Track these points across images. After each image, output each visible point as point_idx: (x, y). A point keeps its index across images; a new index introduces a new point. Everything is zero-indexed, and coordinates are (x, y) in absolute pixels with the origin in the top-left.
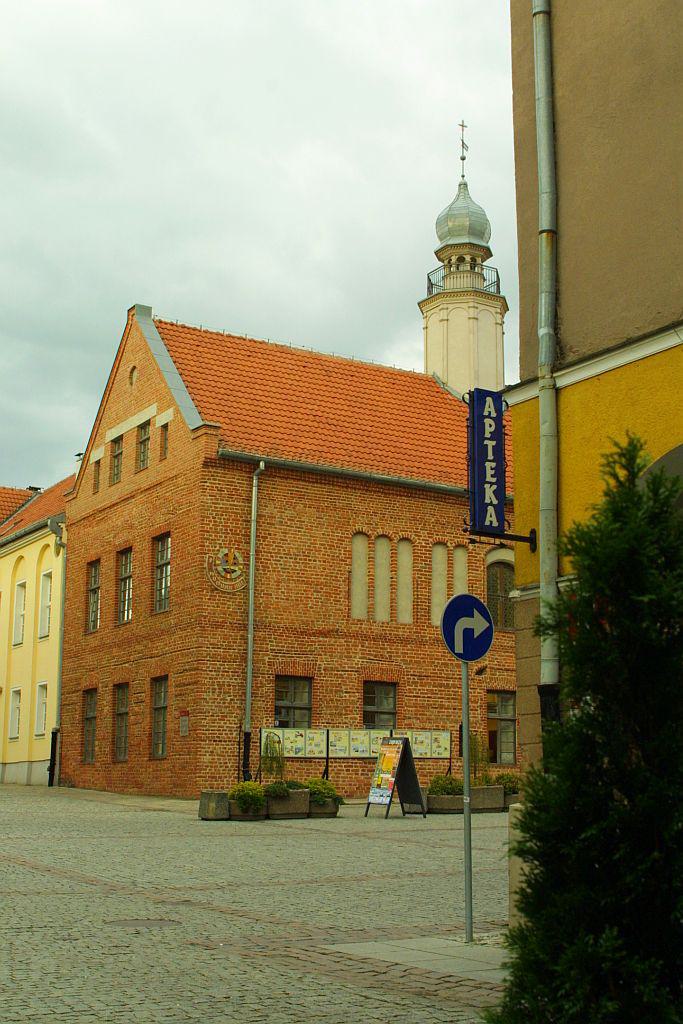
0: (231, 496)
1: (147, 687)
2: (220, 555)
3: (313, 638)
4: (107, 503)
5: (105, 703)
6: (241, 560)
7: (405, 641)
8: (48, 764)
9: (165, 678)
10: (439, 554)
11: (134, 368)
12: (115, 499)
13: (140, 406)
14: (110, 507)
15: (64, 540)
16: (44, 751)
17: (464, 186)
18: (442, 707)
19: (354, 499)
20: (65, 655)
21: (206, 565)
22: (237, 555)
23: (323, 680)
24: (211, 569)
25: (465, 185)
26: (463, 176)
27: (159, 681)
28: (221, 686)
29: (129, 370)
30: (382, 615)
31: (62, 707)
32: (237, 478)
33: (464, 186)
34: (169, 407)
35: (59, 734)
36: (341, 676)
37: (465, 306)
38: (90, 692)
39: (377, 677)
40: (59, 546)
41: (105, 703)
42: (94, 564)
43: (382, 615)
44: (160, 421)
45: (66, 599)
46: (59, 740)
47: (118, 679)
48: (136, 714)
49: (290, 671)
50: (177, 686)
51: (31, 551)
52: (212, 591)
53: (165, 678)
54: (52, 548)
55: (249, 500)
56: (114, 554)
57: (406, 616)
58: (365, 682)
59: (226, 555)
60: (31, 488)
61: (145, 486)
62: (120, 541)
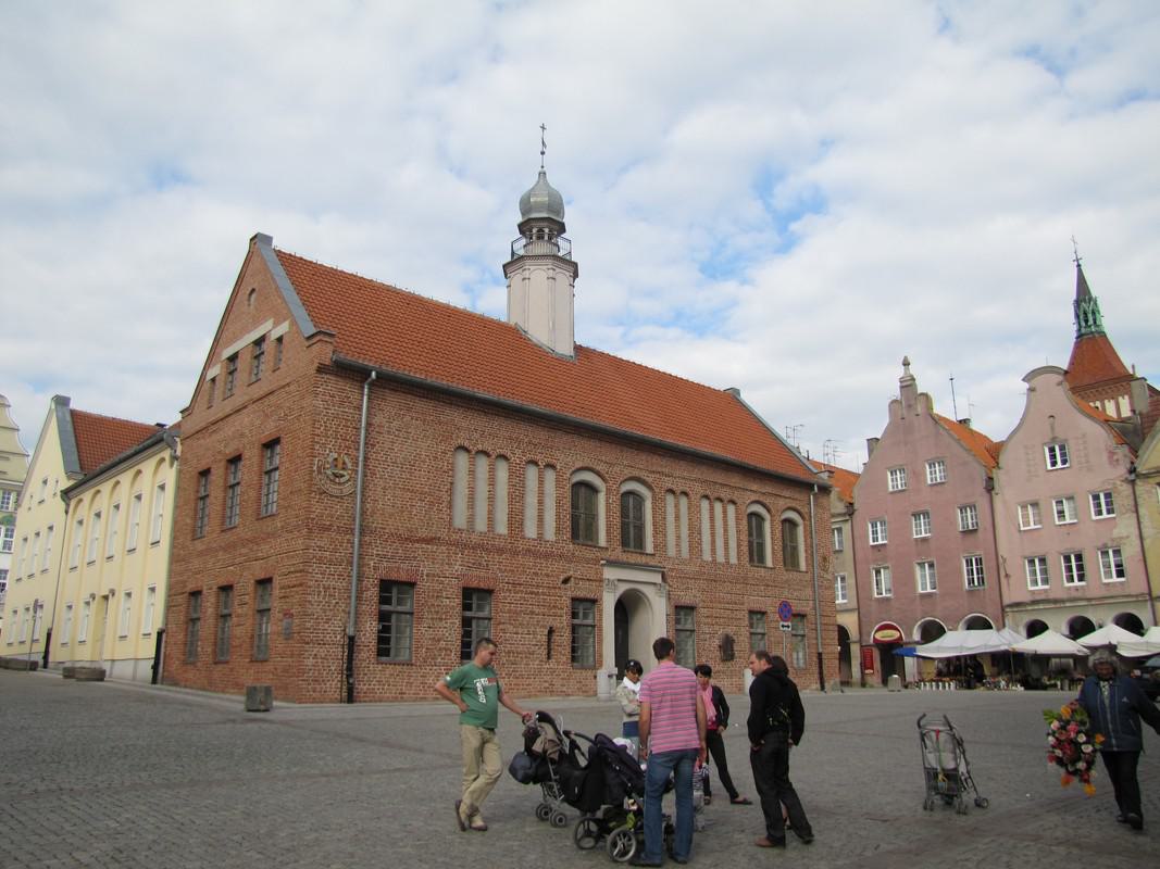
0: (342, 403)
1: (251, 588)
2: (330, 460)
3: (417, 545)
4: (221, 415)
5: (209, 603)
6: (349, 465)
7: (501, 551)
8: (152, 662)
9: (269, 581)
10: (532, 472)
11: (253, 290)
12: (228, 410)
13: (257, 322)
14: (222, 420)
15: (179, 453)
16: (148, 649)
17: (542, 174)
18: (532, 613)
19: (456, 417)
20: (175, 559)
21: (315, 468)
22: (346, 460)
23: (424, 585)
24: (319, 472)
27: (265, 583)
28: (326, 588)
29: (248, 292)
30: (481, 525)
31: (169, 608)
32: (348, 387)
33: (542, 174)
34: (285, 320)
35: (164, 635)
36: (442, 583)
38: (196, 594)
40: (174, 458)
41: (209, 603)
42: (205, 473)
43: (481, 525)
44: (275, 335)
45: (177, 507)
46: (164, 639)
47: (223, 582)
48: (238, 616)
49: (394, 576)
50: (282, 588)
51: (148, 466)
52: (321, 494)
53: (269, 581)
54: (167, 458)
55: (359, 408)
56: (223, 463)
57: (502, 528)
58: (464, 588)
59: (336, 459)
60: (158, 425)
61: (256, 396)
62: (230, 451)
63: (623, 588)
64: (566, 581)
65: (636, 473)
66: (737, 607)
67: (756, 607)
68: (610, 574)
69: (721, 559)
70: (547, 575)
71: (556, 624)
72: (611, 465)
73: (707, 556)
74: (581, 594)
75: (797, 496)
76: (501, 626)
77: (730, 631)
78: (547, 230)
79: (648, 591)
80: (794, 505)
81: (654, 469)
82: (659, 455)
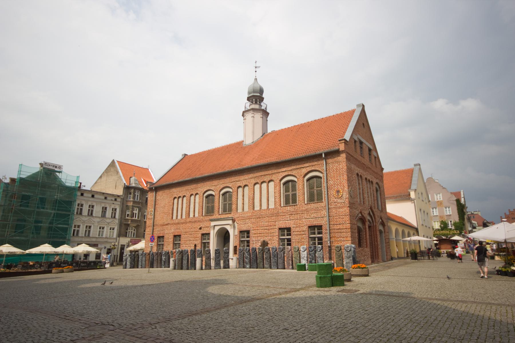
3: (165, 226)
7: (182, 223)
17: (256, 79)
18: (190, 240)
23: (166, 237)
25: (257, 79)
33: (256, 79)
39: (176, 234)
63: (217, 228)
64: (200, 229)
65: (225, 185)
66: (272, 227)
67: (283, 226)
68: (213, 224)
69: (264, 207)
70: (195, 228)
71: (196, 243)
72: (216, 186)
73: (257, 208)
74: (204, 232)
75: (316, 163)
76: (182, 245)
77: (266, 239)
78: (258, 100)
79: (228, 228)
81: (232, 181)
82: (234, 175)
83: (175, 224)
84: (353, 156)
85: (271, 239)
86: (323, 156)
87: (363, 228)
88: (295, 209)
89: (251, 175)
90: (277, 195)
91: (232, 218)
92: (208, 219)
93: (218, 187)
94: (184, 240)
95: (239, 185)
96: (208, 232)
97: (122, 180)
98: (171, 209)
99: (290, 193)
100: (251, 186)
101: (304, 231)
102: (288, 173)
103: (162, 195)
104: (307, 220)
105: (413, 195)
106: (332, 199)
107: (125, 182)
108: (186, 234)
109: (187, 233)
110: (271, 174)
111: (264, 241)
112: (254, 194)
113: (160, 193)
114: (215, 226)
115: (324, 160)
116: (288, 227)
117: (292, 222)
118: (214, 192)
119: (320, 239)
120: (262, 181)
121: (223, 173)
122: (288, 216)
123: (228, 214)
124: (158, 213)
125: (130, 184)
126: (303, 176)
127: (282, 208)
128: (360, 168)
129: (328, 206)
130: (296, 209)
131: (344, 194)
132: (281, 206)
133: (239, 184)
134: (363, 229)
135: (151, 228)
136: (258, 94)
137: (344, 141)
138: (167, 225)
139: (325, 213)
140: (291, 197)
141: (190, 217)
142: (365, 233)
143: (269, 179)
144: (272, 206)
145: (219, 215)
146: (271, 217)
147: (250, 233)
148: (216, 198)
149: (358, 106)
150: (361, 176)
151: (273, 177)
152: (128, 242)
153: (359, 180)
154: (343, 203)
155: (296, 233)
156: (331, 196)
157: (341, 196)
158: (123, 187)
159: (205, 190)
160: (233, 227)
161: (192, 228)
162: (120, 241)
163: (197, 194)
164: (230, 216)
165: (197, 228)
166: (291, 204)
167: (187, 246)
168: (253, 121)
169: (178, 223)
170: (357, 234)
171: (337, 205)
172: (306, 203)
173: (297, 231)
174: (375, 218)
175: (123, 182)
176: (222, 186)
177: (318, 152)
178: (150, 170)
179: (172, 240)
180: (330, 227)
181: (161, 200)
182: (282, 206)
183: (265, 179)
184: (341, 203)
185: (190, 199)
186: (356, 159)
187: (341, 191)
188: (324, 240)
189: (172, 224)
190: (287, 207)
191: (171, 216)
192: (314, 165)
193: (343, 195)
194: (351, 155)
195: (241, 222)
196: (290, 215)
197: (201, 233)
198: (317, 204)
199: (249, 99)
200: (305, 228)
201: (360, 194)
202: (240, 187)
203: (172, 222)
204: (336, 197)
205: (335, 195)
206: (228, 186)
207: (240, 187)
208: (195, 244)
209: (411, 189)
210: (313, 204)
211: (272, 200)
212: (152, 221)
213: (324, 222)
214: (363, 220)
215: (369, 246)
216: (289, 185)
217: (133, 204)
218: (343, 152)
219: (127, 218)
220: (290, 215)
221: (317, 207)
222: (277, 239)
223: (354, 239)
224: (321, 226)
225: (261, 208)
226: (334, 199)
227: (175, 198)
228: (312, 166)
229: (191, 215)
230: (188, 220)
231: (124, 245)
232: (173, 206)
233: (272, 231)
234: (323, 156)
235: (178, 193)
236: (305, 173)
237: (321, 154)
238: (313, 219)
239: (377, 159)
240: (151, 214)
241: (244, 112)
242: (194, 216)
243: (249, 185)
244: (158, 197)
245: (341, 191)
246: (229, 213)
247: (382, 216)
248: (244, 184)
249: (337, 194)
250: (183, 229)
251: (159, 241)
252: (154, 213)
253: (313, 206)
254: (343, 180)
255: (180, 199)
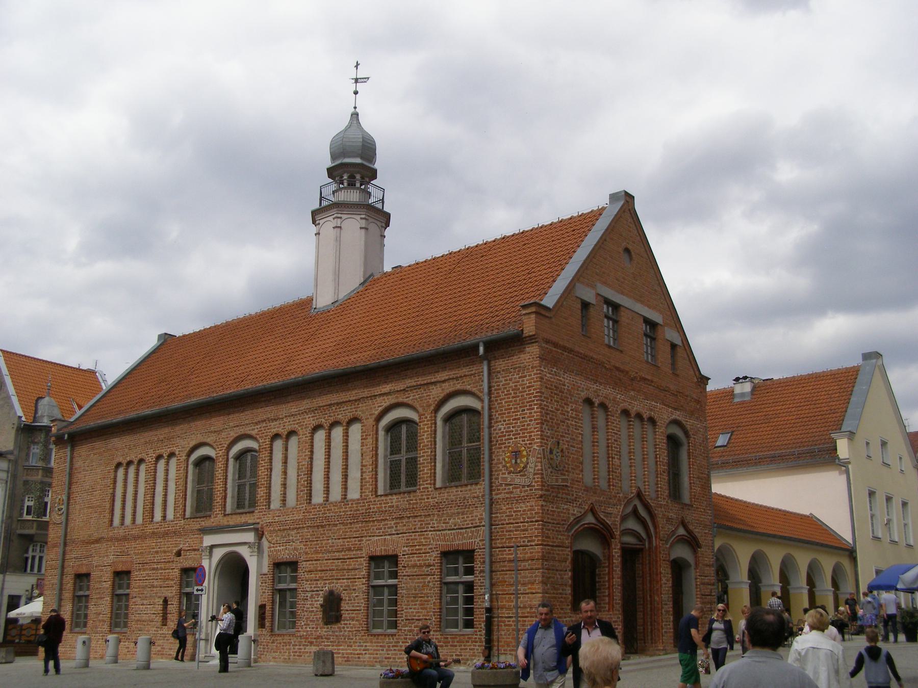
2: (57, 501)
3: (92, 546)
7: (135, 538)
17: (355, 116)
18: (153, 586)
25: (357, 114)
26: (355, 108)
33: (355, 116)
37: (358, 217)
63: (218, 554)
64: (179, 554)
65: (241, 431)
66: (352, 554)
67: (379, 550)
68: (209, 540)
69: (336, 494)
70: (165, 552)
71: (169, 594)
72: (218, 432)
73: (318, 498)
75: (465, 371)
76: (134, 600)
77: (338, 586)
78: (358, 177)
79: (244, 552)
80: (459, 387)
81: (259, 419)
83: (118, 540)
84: (570, 351)
85: (349, 586)
86: (481, 349)
87: (604, 556)
88: (410, 504)
89: (305, 404)
90: (368, 461)
91: (256, 526)
92: (198, 527)
93: (224, 434)
94: (139, 587)
95: (275, 431)
96: (195, 565)
97: (12, 407)
98: (108, 498)
99: (403, 456)
100: (304, 433)
101: (429, 566)
102: (397, 397)
103: (88, 456)
104: (438, 533)
105: (843, 448)
106: (503, 476)
107: (20, 413)
108: (144, 570)
109: (146, 567)
110: (356, 400)
111: (331, 593)
112: (311, 458)
113: (83, 451)
114: (212, 547)
115: (485, 363)
116: (390, 553)
117: (402, 539)
118: (214, 449)
119: (469, 587)
120: (332, 419)
121: (235, 396)
122: (393, 522)
123: (246, 513)
124: (78, 507)
125: (35, 417)
126: (432, 408)
127: (379, 498)
128: (601, 384)
129: (491, 494)
130: (413, 504)
131: (532, 459)
132: (376, 492)
133: (275, 427)
134: (602, 558)
135: (60, 550)
136: (358, 160)
137: (533, 309)
138: (98, 541)
139: (481, 513)
140: (403, 469)
141: (154, 520)
142: (607, 569)
143: (350, 416)
144: (354, 493)
145: (225, 515)
146: (351, 523)
147: (300, 570)
148: (219, 465)
149: (614, 197)
150: (603, 406)
151: (361, 410)
152: (29, 588)
153: (593, 417)
154: (528, 486)
155: (409, 571)
156: (500, 466)
157: (522, 465)
158: (15, 427)
159: (191, 446)
160: (256, 550)
161: (157, 552)
162: (7, 585)
163: (172, 455)
164: (250, 519)
165: (172, 551)
166: (403, 488)
167: (145, 602)
168: (338, 240)
169: (125, 538)
170: (570, 574)
171: (512, 492)
172: (439, 484)
173: (414, 566)
174: (655, 527)
175: (16, 413)
176: (233, 434)
177: (470, 341)
178: (97, 374)
179: (108, 585)
180: (491, 555)
181: (84, 470)
182: (379, 493)
183: (340, 416)
184: (524, 486)
185: (156, 469)
186: (584, 357)
187: (525, 453)
188: (478, 590)
189: (111, 539)
190: (390, 497)
191: (108, 516)
192: (461, 377)
193: (528, 463)
194: (564, 348)
195: (276, 536)
196: (396, 518)
197: (180, 566)
198: (463, 489)
199: (331, 172)
200: (433, 557)
201: (594, 458)
202: (276, 436)
203: (111, 534)
204: (512, 469)
205: (508, 465)
206: (249, 432)
207: (276, 436)
208: (166, 598)
209: (842, 430)
210: (454, 490)
211: (355, 474)
212: (61, 532)
213: (477, 540)
214: (602, 533)
215: (618, 607)
216: (400, 432)
217: (43, 476)
218: (532, 339)
219: (26, 517)
220: (396, 518)
221: (465, 498)
222: (364, 587)
223: (555, 589)
224: (473, 551)
225: (327, 497)
226: (507, 475)
227: (119, 465)
228: (457, 379)
229: (158, 517)
230: (149, 529)
231: (19, 597)
232: (114, 488)
233: (353, 564)
234: (481, 349)
235: (126, 450)
236: (438, 399)
237: (475, 347)
238: (453, 532)
239: (680, 352)
240: (59, 510)
241: (314, 213)
242: (164, 517)
243: (301, 432)
244: (78, 463)
245: (525, 453)
246: (249, 513)
247: (688, 519)
248: (289, 428)
249: (513, 461)
250: (136, 554)
251: (78, 587)
252: (68, 509)
253: (455, 493)
254: (531, 421)
255: (132, 470)
